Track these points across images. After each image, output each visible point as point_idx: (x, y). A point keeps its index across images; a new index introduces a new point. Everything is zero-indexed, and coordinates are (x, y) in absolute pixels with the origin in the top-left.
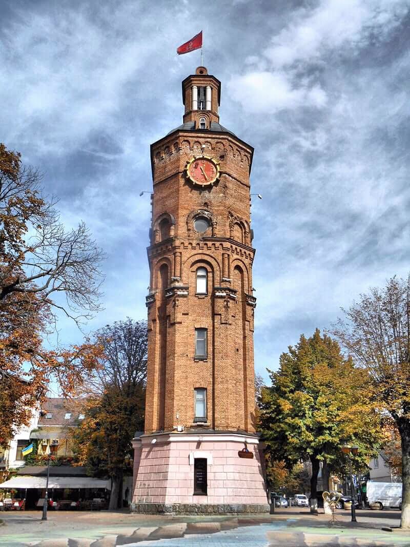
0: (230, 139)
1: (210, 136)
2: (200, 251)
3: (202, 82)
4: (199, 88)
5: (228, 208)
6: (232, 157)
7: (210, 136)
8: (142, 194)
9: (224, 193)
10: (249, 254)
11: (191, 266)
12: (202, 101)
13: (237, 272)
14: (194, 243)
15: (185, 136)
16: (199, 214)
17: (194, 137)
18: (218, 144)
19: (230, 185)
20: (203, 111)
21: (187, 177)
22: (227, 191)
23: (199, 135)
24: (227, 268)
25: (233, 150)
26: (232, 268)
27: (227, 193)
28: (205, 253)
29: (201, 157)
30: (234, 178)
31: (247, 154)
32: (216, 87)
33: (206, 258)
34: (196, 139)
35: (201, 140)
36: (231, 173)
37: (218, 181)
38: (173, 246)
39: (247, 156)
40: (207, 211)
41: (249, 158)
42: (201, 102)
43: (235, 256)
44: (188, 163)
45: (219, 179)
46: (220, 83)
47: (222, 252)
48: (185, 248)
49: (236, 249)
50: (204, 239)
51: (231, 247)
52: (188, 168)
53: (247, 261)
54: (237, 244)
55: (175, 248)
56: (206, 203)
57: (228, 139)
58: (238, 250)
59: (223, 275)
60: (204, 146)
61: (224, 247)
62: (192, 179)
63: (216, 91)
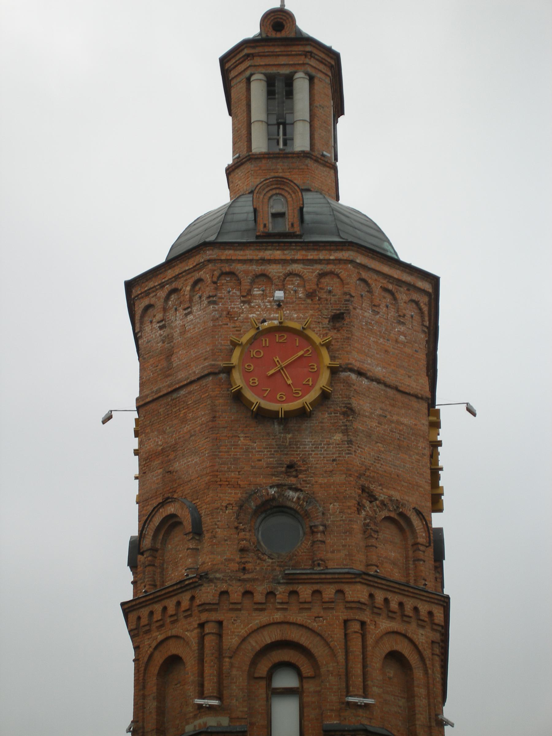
0: (360, 259)
1: (299, 256)
2: (278, 616)
3: (282, 60)
4: (270, 81)
5: (359, 478)
6: (368, 314)
7: (299, 256)
8: (108, 418)
9: (345, 432)
10: (430, 614)
11: (254, 662)
12: (281, 124)
13: (391, 672)
14: (260, 591)
15: (229, 261)
16: (273, 499)
17: (250, 261)
18: (325, 281)
19: (362, 405)
20: (282, 153)
21: (234, 389)
22: (357, 425)
23: (268, 254)
24: (360, 666)
25: (370, 292)
26: (376, 663)
27: (356, 431)
28: (292, 619)
29: (276, 322)
30: (378, 381)
31: (416, 296)
32: (322, 67)
33: (295, 635)
34: (256, 269)
35: (274, 270)
36: (365, 367)
37: (325, 396)
38: (198, 602)
39: (417, 303)
40: (296, 490)
41: (425, 309)
42: (278, 124)
43: (385, 625)
44: (235, 344)
45: (329, 389)
46: (336, 57)
47: (342, 614)
48: (236, 608)
49: (386, 600)
50: (291, 579)
51: (371, 596)
52: (235, 359)
53: (423, 637)
54: (390, 586)
55: (205, 607)
56: (291, 466)
57: (352, 262)
58: (394, 605)
59: (347, 687)
60: (279, 294)
61: (349, 599)
62: (249, 395)
63: (324, 87)
